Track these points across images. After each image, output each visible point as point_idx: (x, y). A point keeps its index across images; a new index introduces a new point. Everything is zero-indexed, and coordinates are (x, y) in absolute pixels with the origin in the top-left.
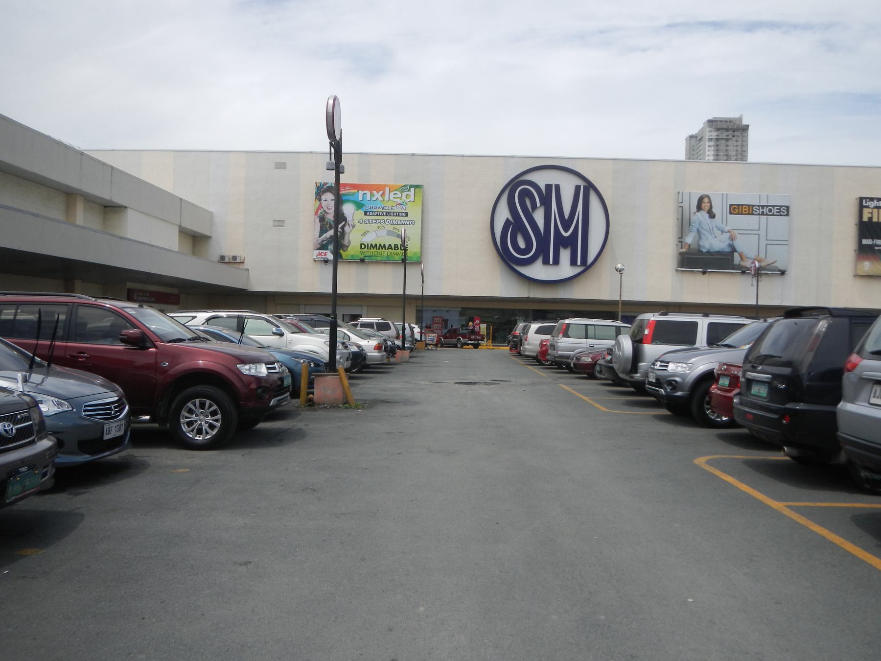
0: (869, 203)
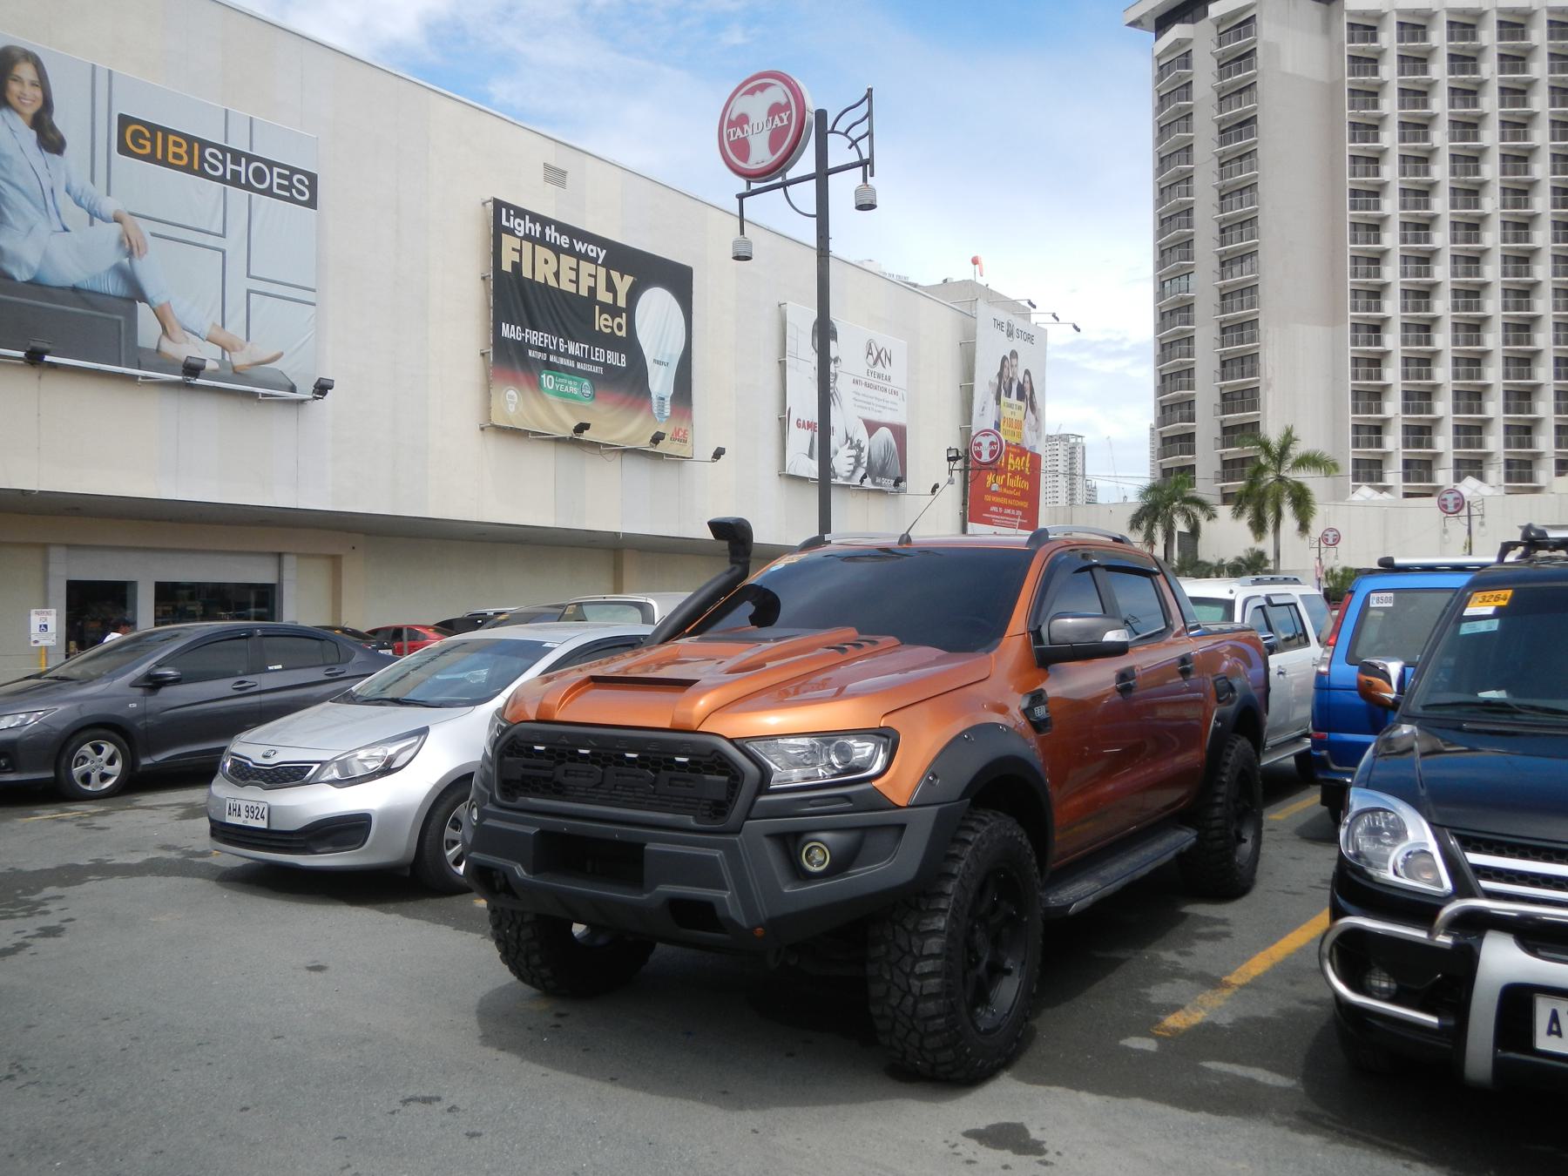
0: (514, 223)
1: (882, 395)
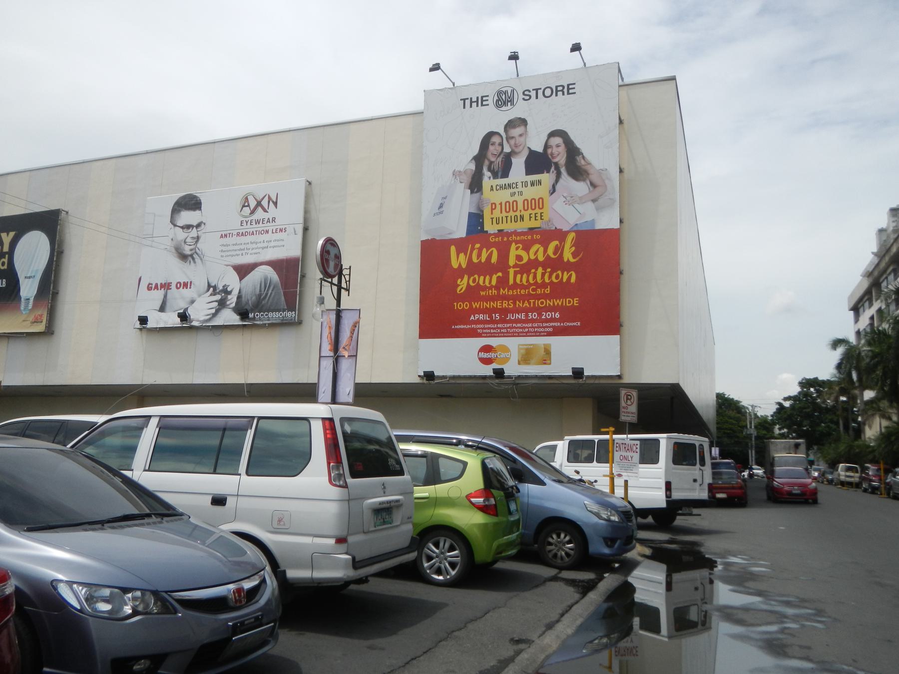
1: (265, 237)
